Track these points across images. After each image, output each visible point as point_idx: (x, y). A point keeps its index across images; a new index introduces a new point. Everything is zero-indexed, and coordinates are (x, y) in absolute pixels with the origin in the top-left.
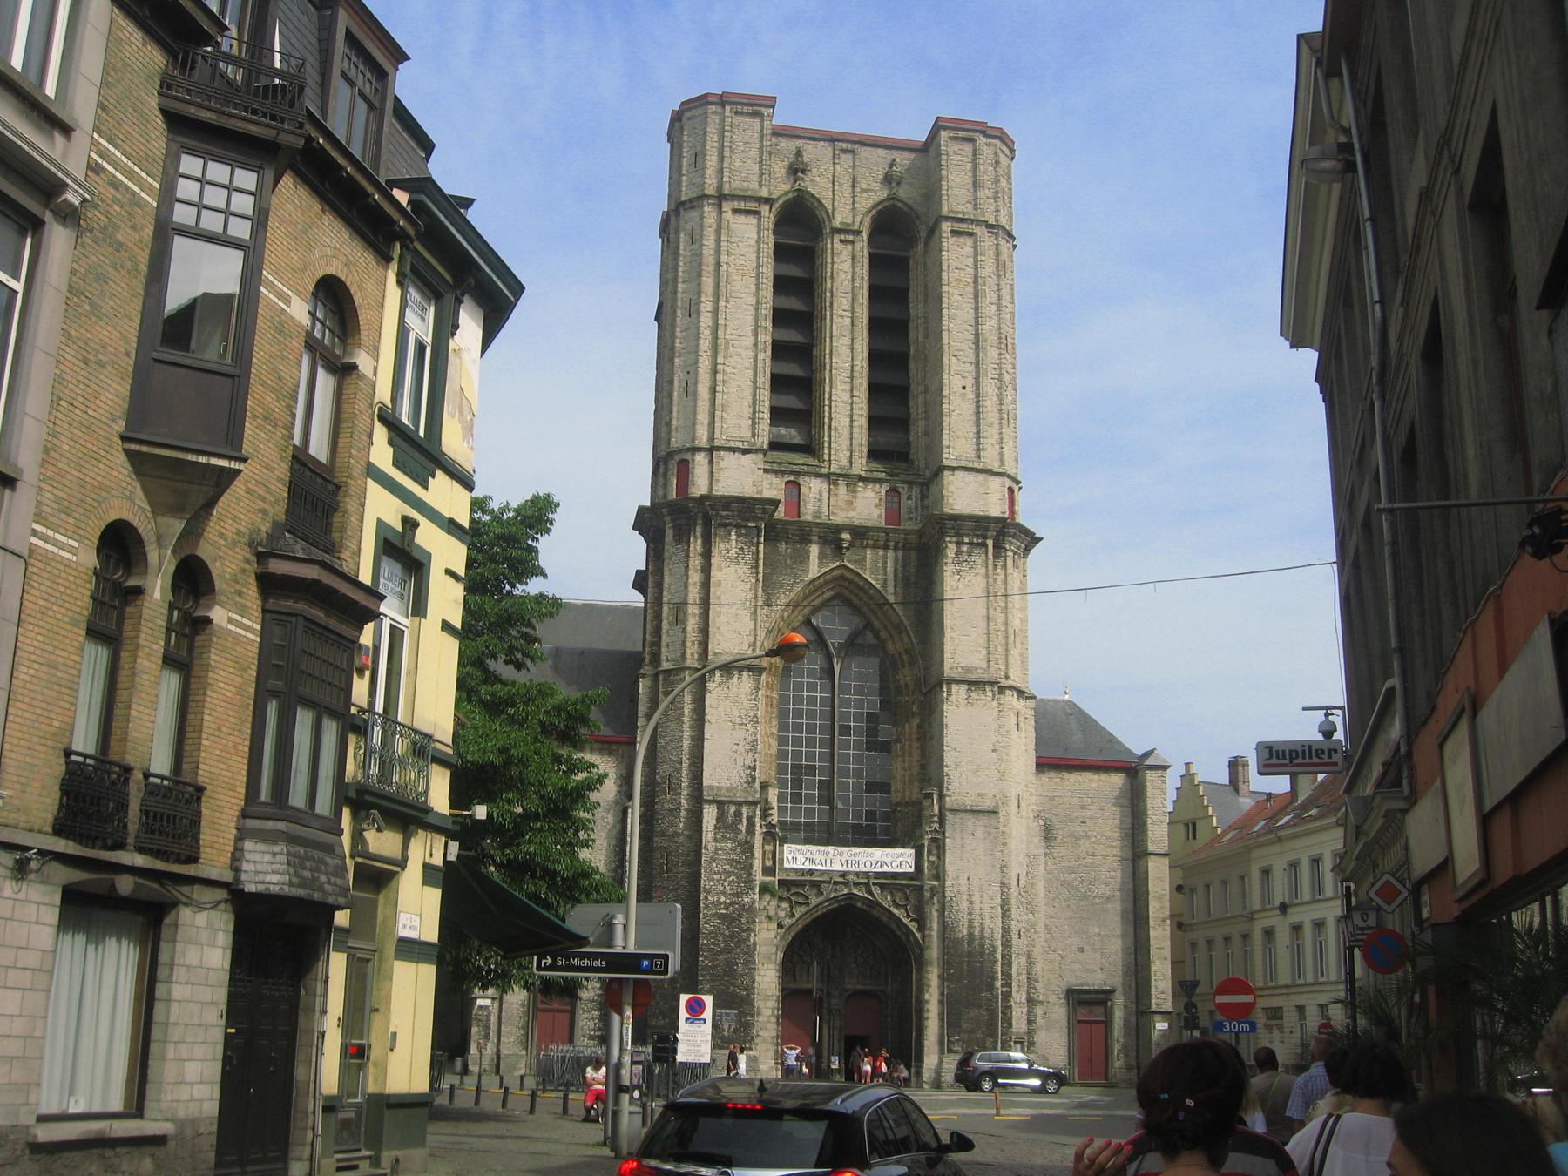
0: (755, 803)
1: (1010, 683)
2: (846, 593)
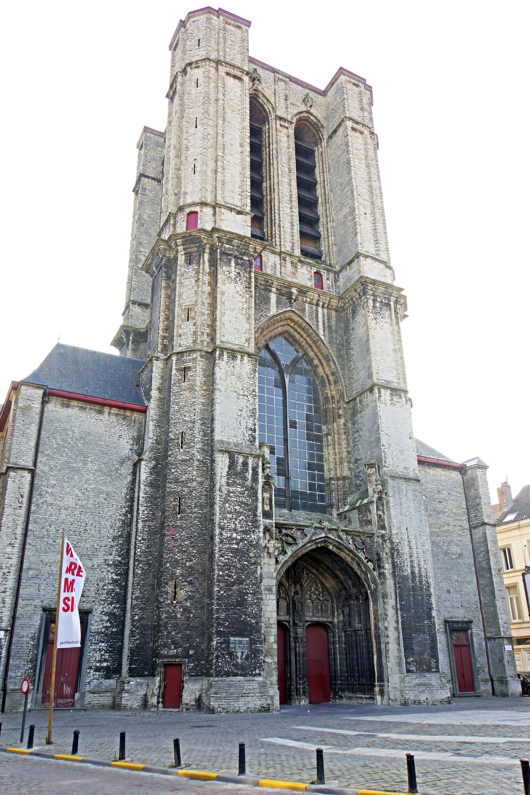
0: (257, 457)
2: (292, 330)
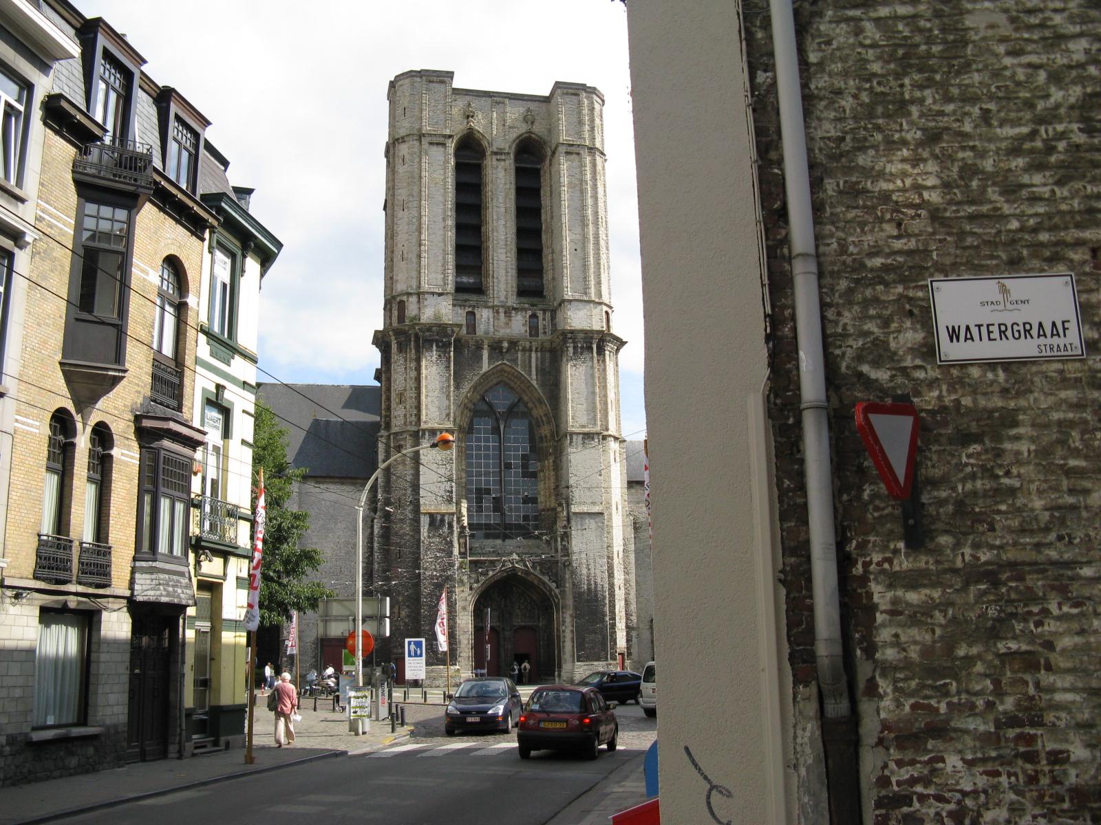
0: (453, 514)
1: (610, 433)
2: (505, 379)
